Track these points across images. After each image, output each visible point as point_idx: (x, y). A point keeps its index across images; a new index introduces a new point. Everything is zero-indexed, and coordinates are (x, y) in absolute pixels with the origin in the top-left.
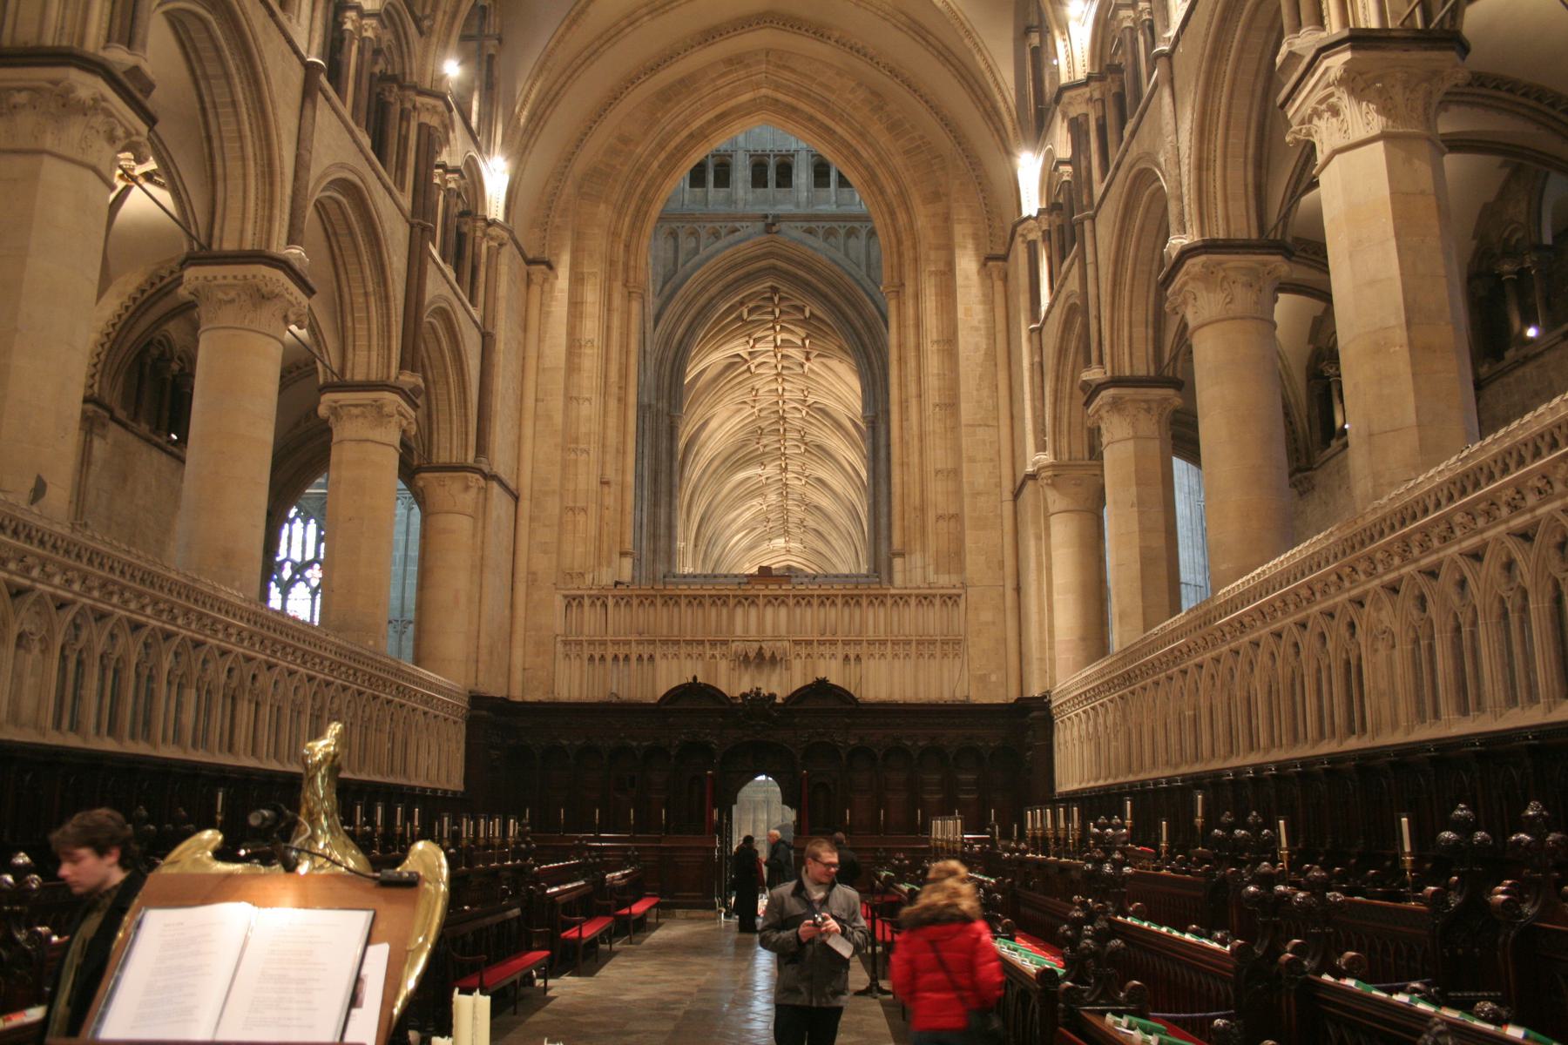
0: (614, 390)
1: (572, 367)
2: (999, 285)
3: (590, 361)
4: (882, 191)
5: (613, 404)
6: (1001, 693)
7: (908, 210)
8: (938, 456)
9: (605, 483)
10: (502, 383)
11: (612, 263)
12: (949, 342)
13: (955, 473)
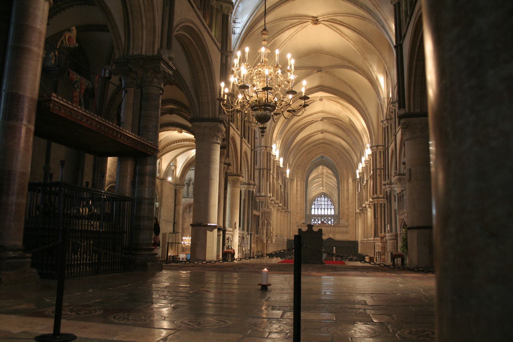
0: (302, 196)
1: (297, 194)
2: (355, 184)
3: (299, 193)
4: (339, 166)
5: (302, 198)
6: (352, 239)
7: (343, 170)
8: (346, 207)
9: (301, 209)
10: (289, 199)
11: (301, 178)
12: (348, 190)
13: (348, 209)
